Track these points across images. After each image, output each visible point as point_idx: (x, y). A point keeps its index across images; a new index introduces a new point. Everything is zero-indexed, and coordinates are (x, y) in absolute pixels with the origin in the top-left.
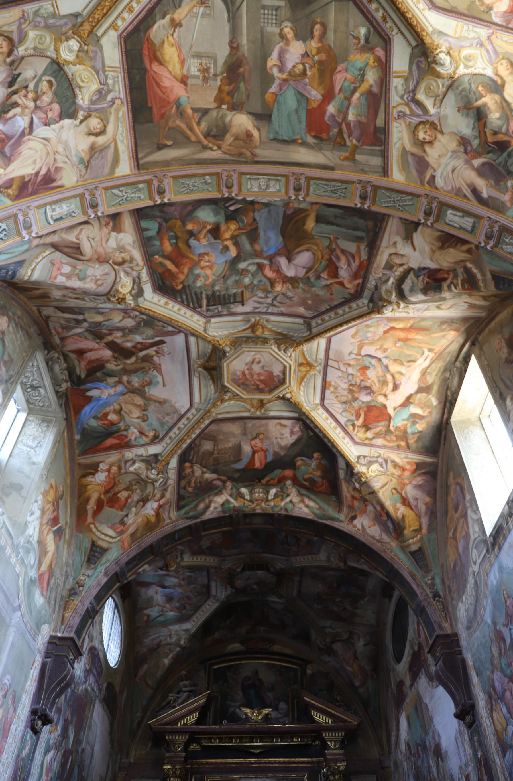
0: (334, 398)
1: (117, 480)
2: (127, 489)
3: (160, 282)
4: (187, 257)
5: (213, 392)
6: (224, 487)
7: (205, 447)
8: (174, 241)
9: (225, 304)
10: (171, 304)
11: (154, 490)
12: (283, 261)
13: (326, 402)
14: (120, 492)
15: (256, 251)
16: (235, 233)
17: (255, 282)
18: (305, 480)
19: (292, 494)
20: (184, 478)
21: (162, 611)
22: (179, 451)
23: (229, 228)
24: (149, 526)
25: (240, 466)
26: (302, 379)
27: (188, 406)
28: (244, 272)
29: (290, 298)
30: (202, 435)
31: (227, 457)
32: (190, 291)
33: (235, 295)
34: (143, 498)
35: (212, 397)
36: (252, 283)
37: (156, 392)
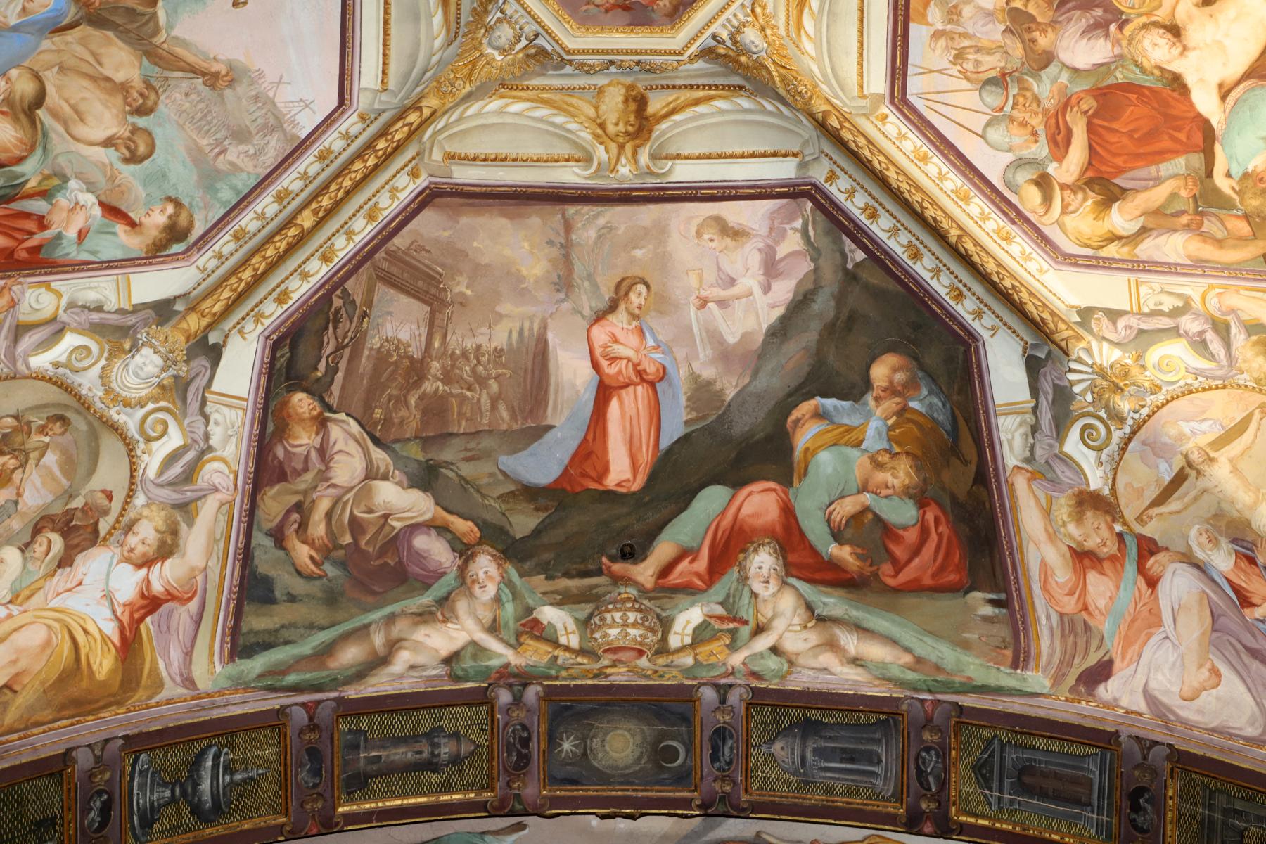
0: (945, 64)
5: (438, 43)
7: (389, 331)
11: (130, 495)
13: (915, 85)
18: (837, 536)
19: (779, 625)
20: (281, 475)
22: (274, 313)
25: (542, 465)
30: (380, 255)
31: (485, 399)
34: (70, 514)
35: (435, 59)
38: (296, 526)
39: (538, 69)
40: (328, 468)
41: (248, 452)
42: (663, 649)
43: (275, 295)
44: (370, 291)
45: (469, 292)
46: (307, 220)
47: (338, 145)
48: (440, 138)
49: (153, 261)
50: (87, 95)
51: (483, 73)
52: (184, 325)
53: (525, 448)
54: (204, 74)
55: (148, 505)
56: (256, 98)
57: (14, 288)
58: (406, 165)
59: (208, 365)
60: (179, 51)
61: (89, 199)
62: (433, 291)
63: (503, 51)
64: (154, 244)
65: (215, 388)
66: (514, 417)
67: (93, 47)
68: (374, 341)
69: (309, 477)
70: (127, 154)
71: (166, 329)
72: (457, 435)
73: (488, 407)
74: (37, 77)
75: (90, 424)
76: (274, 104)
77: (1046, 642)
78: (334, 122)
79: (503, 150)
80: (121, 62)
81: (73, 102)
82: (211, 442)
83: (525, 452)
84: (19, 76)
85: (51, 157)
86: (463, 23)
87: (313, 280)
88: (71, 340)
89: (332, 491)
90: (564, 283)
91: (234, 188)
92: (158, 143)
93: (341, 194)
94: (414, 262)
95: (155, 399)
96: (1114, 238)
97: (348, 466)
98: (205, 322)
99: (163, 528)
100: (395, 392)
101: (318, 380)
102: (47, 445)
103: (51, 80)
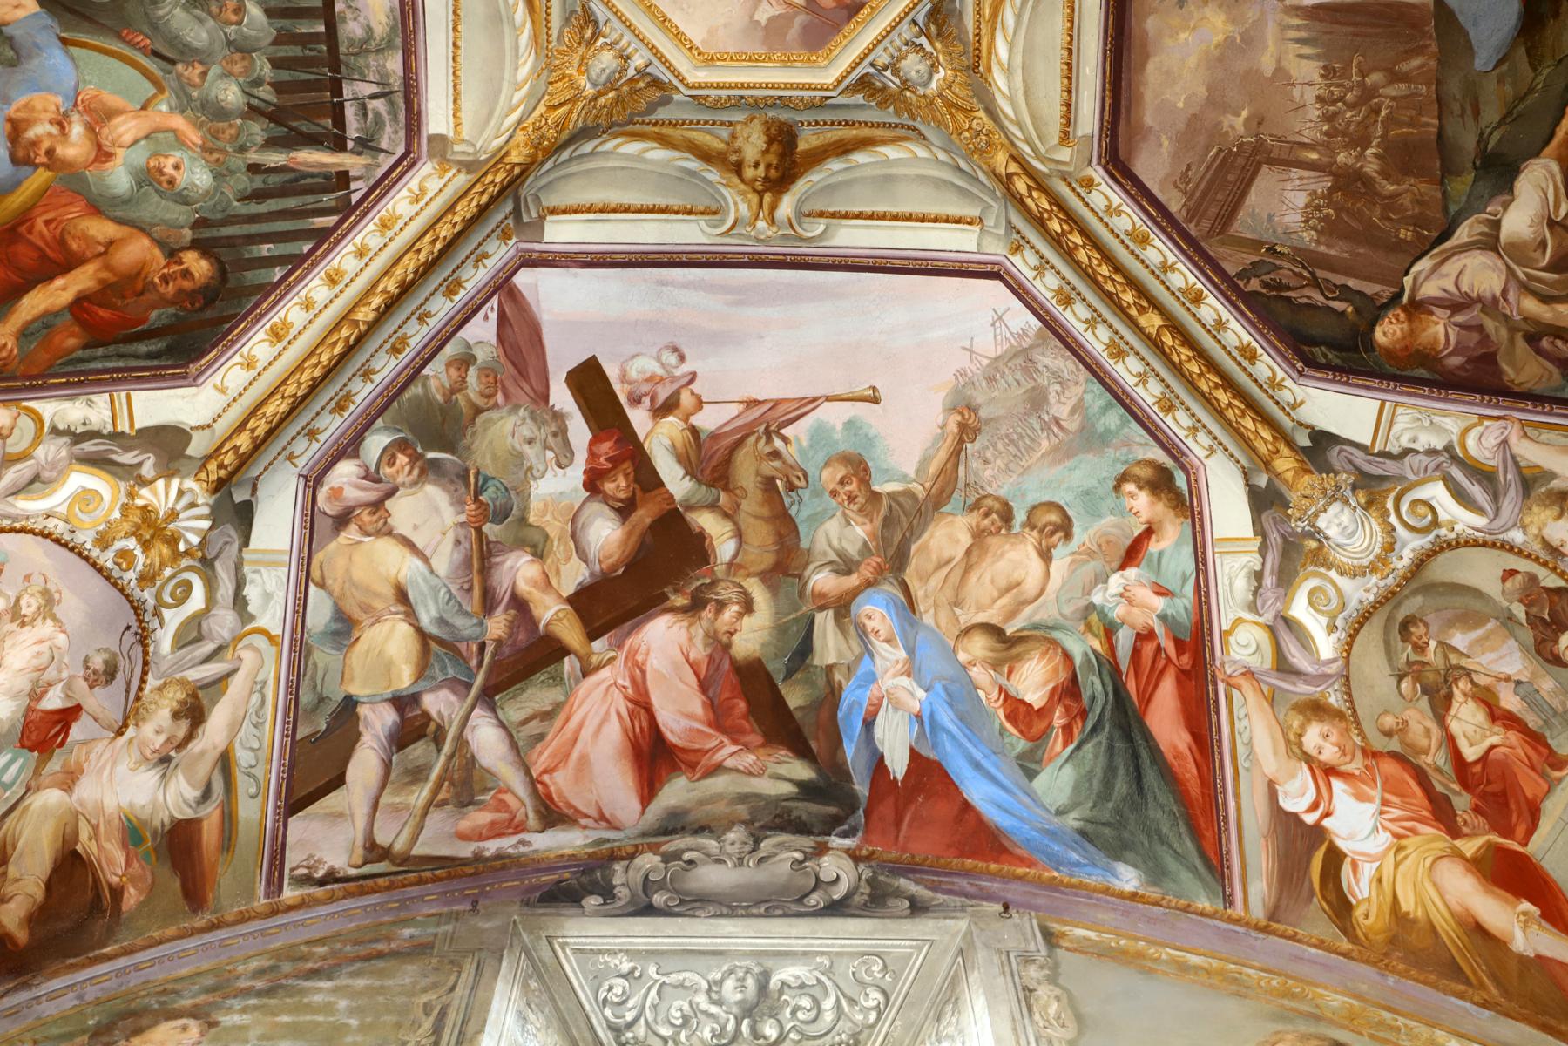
1: (1379, 743)
2: (1441, 704)
3: (142, 348)
4: (25, 216)
5: (922, 153)
7: (1293, 219)
9: (334, 62)
10: (291, 311)
11: (1511, 548)
14: (1451, 741)
22: (1267, 365)
30: (1192, 229)
31: (1393, 91)
35: (942, 156)
37: (905, 447)
38: (1559, 343)
39: (953, 22)
40: (1479, 300)
41: (1454, 401)
43: (1245, 363)
44: (1241, 243)
45: (1245, 113)
46: (1151, 321)
47: (1052, 281)
48: (1043, 151)
49: (1196, 510)
50: (987, 577)
51: (961, 93)
52: (1289, 475)
53: (1466, 34)
54: (961, 441)
55: (1524, 528)
56: (991, 379)
57: (1229, 672)
58: (1078, 195)
59: (1337, 448)
60: (933, 469)
61: (1116, 581)
62: (1240, 161)
63: (933, 68)
64: (1174, 508)
65: (1368, 442)
66: (1420, 51)
67: (930, 567)
68: (1308, 237)
69: (1490, 325)
70: (1060, 534)
71: (1293, 497)
72: (1441, 129)
73: (1404, 86)
74: (967, 631)
75: (1415, 592)
76: (997, 359)
78: (1020, 285)
79: (1058, 68)
80: (947, 536)
81: (996, 594)
82: (1439, 447)
83: (1472, 34)
84: (965, 650)
85: (1061, 621)
86: (897, 121)
87: (1225, 315)
88: (1300, 609)
89: (1511, 296)
91: (1105, 410)
92: (1046, 499)
93: (1118, 278)
94: (1202, 186)
95: (1384, 514)
97: (1480, 274)
98: (1284, 450)
99: (1556, 510)
100: (1378, 211)
101: (1357, 310)
102: (1441, 644)
103: (968, 617)
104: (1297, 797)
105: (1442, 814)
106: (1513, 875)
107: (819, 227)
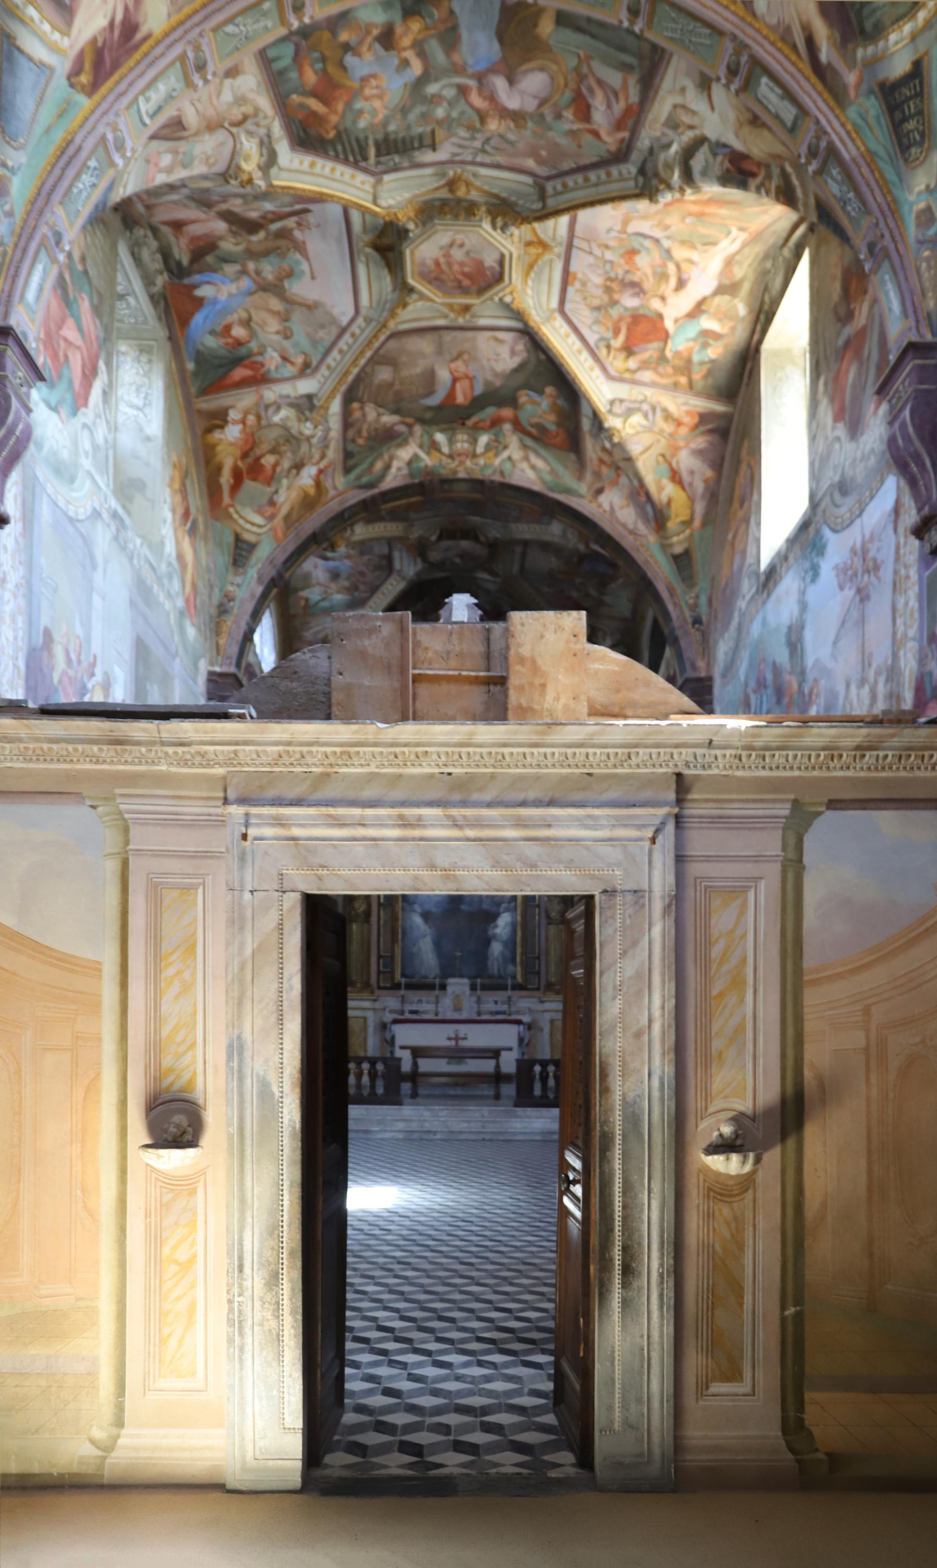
1: (256, 436)
2: (273, 451)
6: (411, 433)
8: (319, 66)
12: (500, 83)
13: (568, 307)
14: (263, 456)
15: (454, 64)
16: (420, 37)
17: (454, 114)
18: (532, 426)
21: (326, 592)
22: (343, 388)
23: (408, 28)
24: (308, 503)
25: (435, 400)
26: (531, 266)
27: (351, 312)
28: (436, 99)
29: (512, 143)
32: (348, 136)
33: (421, 137)
36: (448, 116)
37: (300, 288)
42: (475, 456)
61: (275, 355)
74: (247, 311)
77: (589, 476)
80: (276, 304)
88: (284, 413)
90: (440, 351)
96: (628, 370)
104: (233, 415)
105: (245, 455)
106: (238, 477)
107: (363, 259)
